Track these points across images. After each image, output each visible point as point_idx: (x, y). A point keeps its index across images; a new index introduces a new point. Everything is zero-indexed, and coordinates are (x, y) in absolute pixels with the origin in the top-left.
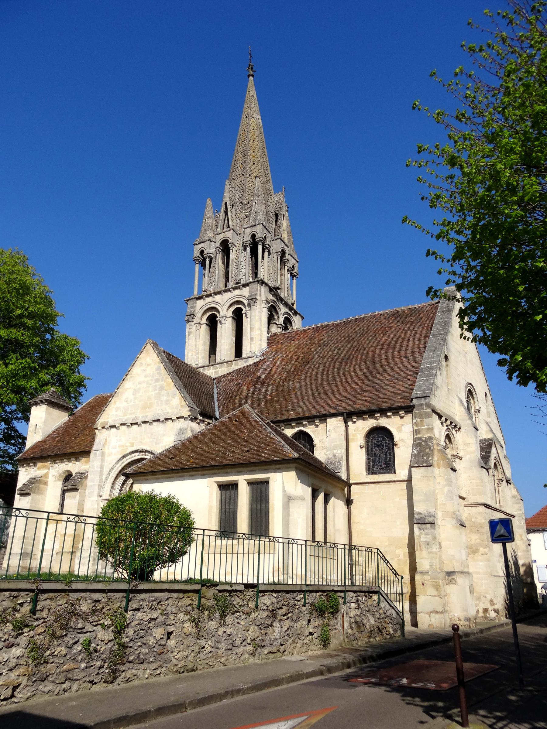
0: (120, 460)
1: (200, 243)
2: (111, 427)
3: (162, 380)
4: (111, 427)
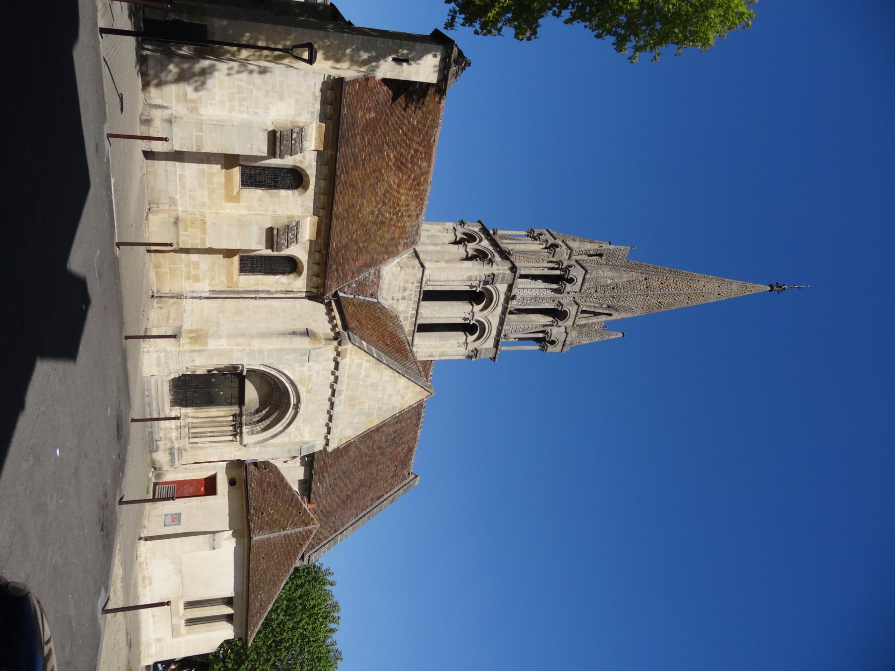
1: (584, 279)
2: (337, 364)
3: (378, 415)
4: (337, 364)
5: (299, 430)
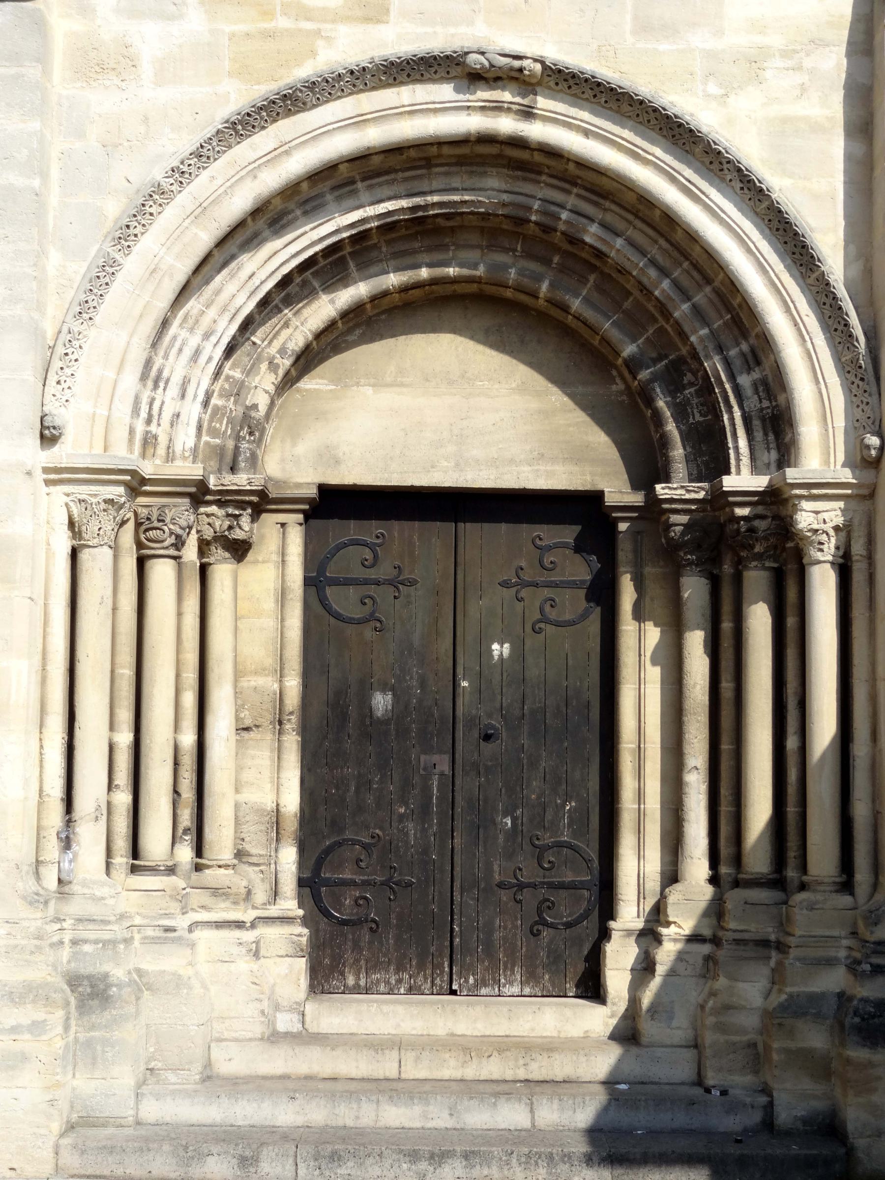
0: (243, 125)
5: (754, 64)
